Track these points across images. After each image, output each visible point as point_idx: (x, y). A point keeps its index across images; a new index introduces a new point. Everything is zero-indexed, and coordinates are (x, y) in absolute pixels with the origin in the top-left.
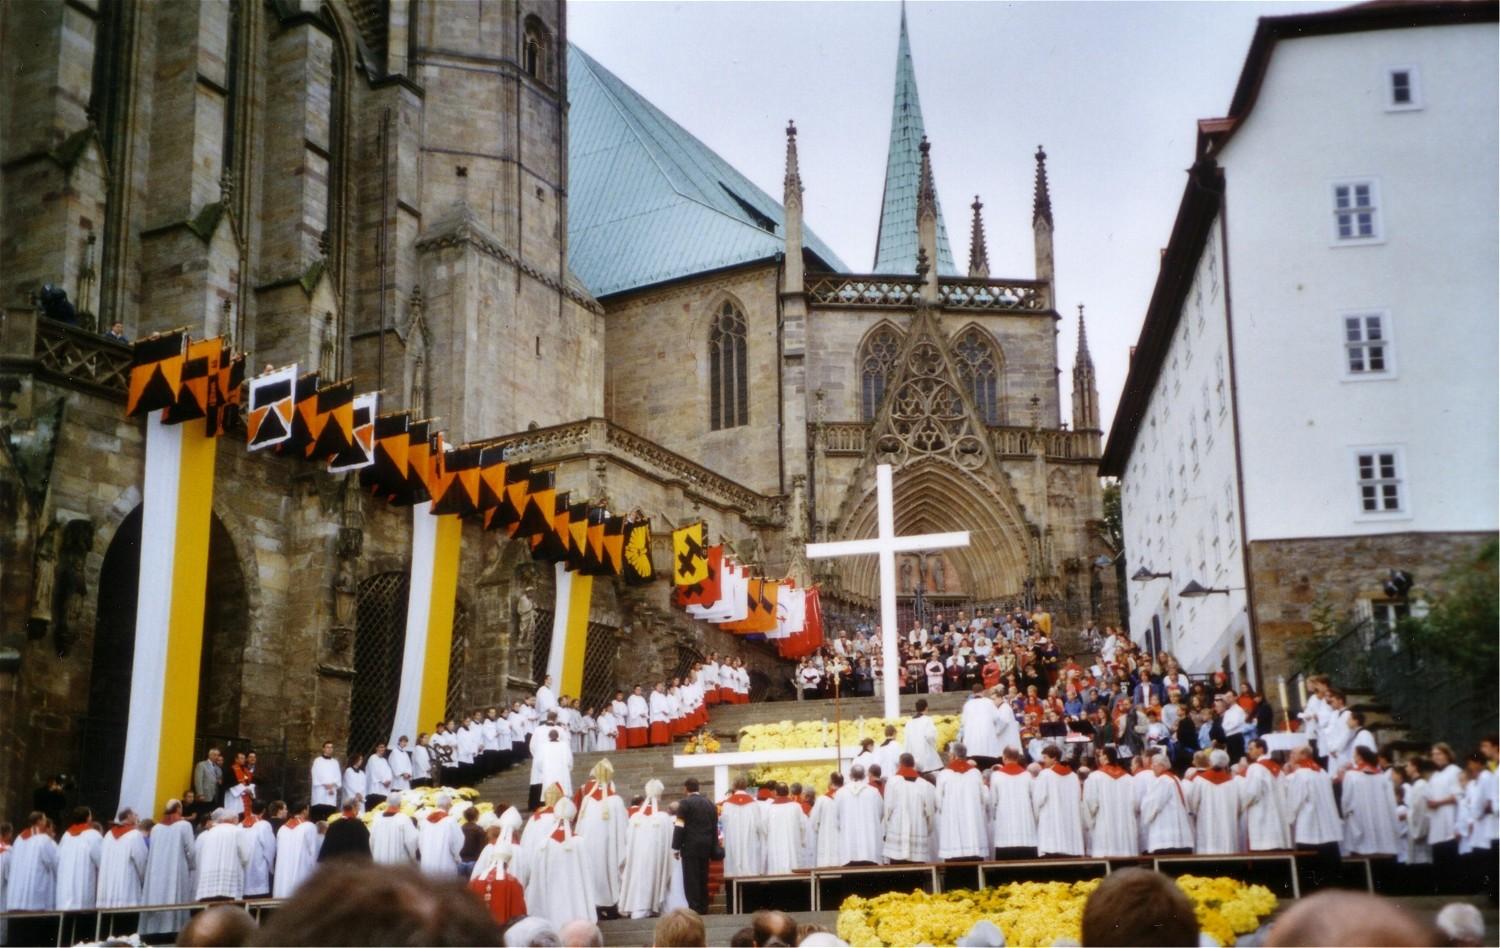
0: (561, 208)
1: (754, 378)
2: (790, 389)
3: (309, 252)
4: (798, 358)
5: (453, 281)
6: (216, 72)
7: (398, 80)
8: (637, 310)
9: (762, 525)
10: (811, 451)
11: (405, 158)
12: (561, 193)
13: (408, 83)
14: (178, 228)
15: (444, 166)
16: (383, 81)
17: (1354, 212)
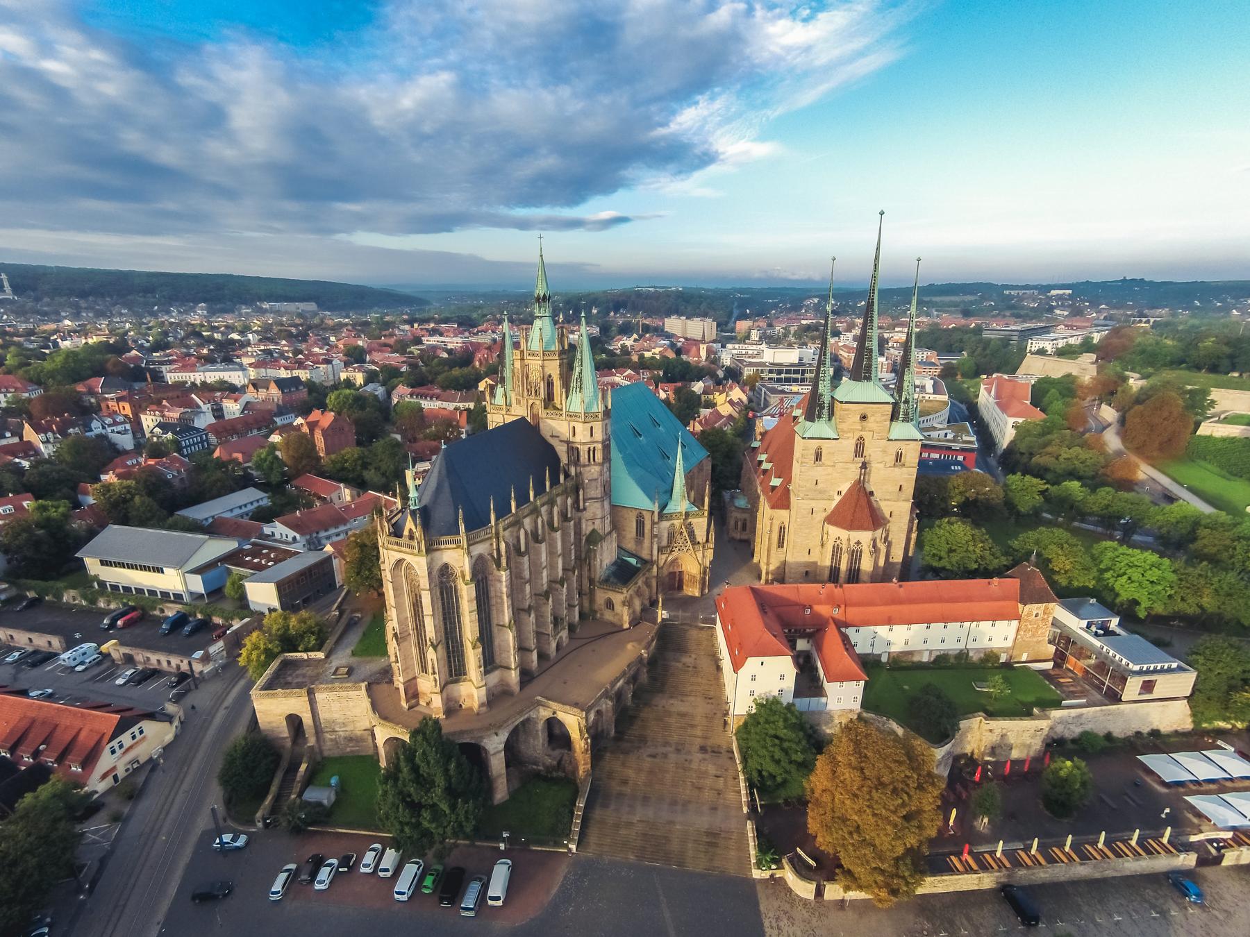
4: (656, 536)
11: (584, 526)
15: (590, 523)
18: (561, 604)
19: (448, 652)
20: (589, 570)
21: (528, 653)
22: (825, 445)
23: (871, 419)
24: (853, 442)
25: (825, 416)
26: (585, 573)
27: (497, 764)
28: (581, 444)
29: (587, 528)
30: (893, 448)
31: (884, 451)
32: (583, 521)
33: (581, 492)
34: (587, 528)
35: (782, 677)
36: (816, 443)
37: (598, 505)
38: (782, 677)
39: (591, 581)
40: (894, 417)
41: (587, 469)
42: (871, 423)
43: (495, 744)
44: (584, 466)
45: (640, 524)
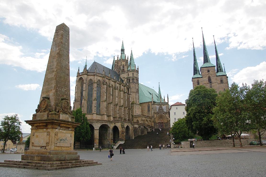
5: (133, 106)
8: (143, 104)
9: (151, 119)
10: (154, 114)
11: (130, 99)
12: (139, 99)
14: (121, 106)
15: (132, 99)
17: (175, 113)
19: (88, 105)
20: (132, 112)
21: (110, 117)
23: (210, 71)
25: (198, 73)
26: (131, 113)
27: (96, 134)
28: (130, 77)
30: (219, 78)
33: (130, 89)
36: (196, 80)
39: (132, 116)
40: (218, 71)
41: (132, 84)
42: (211, 72)
43: (97, 126)
44: (131, 83)
45: (149, 107)
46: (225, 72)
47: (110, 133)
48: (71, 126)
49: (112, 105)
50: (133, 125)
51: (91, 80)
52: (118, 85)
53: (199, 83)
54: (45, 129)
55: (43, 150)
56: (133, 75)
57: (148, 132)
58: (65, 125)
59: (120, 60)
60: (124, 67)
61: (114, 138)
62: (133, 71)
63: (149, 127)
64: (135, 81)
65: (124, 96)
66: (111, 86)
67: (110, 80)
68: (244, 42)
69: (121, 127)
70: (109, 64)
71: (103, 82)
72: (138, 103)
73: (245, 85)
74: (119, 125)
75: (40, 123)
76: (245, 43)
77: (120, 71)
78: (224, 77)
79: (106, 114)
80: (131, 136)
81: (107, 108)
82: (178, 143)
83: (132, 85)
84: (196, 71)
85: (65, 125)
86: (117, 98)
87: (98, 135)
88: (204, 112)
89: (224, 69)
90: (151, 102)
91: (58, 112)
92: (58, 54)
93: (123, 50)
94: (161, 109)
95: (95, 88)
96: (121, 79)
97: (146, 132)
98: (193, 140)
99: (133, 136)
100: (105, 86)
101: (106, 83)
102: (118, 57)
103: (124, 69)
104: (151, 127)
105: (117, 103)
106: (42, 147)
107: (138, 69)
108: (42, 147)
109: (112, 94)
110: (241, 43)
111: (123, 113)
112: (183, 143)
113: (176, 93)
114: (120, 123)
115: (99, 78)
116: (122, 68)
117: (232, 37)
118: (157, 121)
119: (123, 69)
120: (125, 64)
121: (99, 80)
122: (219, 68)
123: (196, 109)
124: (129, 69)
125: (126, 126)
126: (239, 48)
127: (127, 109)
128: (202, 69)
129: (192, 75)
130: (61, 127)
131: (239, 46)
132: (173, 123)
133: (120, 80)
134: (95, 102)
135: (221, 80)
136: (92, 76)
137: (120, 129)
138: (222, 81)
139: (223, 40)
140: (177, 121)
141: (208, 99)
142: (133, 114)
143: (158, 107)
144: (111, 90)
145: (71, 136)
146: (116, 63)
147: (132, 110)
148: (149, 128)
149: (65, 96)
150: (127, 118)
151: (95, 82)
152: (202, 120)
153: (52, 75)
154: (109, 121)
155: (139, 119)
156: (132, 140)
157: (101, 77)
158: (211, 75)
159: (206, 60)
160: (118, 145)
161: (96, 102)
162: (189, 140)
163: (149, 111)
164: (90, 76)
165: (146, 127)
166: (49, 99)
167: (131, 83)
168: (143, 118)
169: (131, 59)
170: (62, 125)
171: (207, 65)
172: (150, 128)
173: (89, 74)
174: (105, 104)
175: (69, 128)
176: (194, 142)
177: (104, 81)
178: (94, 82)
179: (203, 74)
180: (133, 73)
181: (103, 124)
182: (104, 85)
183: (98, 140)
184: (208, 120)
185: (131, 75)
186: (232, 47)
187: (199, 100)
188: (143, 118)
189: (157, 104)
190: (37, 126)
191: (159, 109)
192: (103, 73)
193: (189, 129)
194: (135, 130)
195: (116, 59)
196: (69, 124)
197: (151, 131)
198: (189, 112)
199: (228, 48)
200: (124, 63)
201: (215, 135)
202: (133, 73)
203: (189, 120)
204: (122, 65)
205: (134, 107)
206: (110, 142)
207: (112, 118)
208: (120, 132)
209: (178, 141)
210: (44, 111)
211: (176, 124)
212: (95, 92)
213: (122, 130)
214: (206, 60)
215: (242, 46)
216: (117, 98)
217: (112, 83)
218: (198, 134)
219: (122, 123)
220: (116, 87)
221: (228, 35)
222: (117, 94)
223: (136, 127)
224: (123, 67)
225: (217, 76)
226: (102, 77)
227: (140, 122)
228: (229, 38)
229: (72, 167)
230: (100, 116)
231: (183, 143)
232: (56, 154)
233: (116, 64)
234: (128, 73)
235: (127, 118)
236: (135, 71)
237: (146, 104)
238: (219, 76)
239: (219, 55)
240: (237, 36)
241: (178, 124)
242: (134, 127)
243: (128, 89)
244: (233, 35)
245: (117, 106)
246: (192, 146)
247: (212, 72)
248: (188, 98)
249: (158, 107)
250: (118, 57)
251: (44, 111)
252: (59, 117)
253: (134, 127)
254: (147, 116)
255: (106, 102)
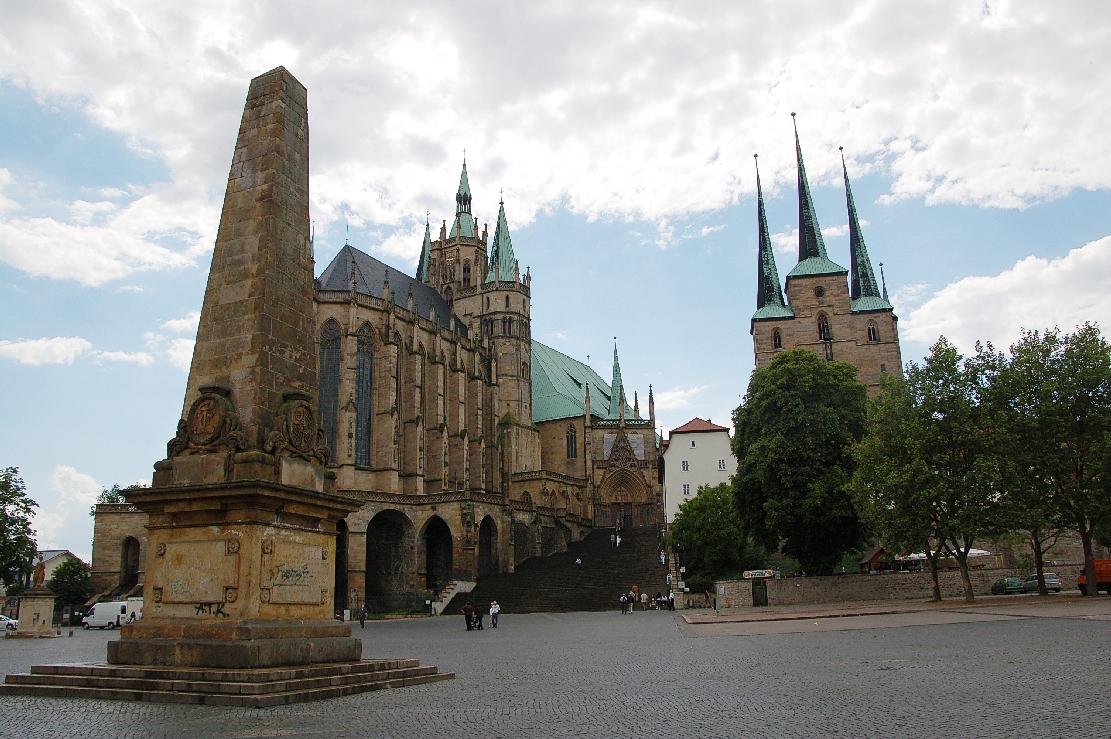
0: (531, 409)
1: (578, 446)
2: (588, 452)
3: (480, 433)
6: (462, 399)
7: (494, 385)
9: (580, 487)
12: (531, 405)
13: (496, 385)
14: (456, 435)
15: (504, 404)
16: (490, 384)
17: (685, 466)
18: (460, 464)
21: (411, 481)
22: (780, 325)
23: (828, 293)
24: (814, 319)
26: (498, 465)
28: (495, 313)
29: (500, 410)
30: (862, 323)
31: (851, 327)
32: (496, 398)
33: (494, 364)
34: (500, 410)
35: (722, 464)
36: (771, 325)
37: (513, 384)
38: (722, 464)
39: (503, 475)
40: (856, 295)
42: (828, 298)
44: (498, 337)
45: (571, 440)
46: (886, 296)
47: (412, 548)
48: (324, 515)
49: (420, 429)
50: (510, 514)
51: (332, 320)
52: (445, 346)
53: (780, 341)
54: (215, 529)
55: (210, 619)
56: (507, 306)
57: (569, 544)
58: (301, 511)
59: (452, 239)
60: (469, 272)
61: (429, 566)
62: (509, 285)
63: (578, 523)
64: (515, 328)
65: (471, 393)
66: (415, 347)
67: (411, 322)
68: (951, 177)
69: (458, 522)
70: (404, 254)
71: (383, 330)
72: (525, 420)
73: (985, 349)
74: (450, 513)
75: (191, 501)
76: (954, 182)
77: (451, 285)
78: (883, 316)
79: (394, 466)
80: (501, 559)
81: (401, 437)
82: (701, 588)
83: (504, 348)
84: (766, 292)
85: (301, 511)
86: (440, 402)
87: (363, 557)
88: (810, 461)
89: (884, 289)
90: (584, 416)
91: (273, 452)
92: (267, 198)
93: (464, 199)
94: (622, 448)
95: (352, 355)
96: (457, 320)
97: (564, 543)
98: (767, 573)
99: (512, 560)
100: (393, 349)
101: (397, 334)
102: (443, 229)
103: (469, 280)
104: (584, 522)
105: (441, 420)
106: (205, 604)
107: (528, 278)
108: (202, 606)
109: (419, 382)
110: (940, 179)
111: (466, 465)
112: (722, 588)
113: (690, 383)
114: (456, 505)
115: (367, 315)
116: (459, 275)
117: (903, 153)
118: (607, 498)
119: (467, 280)
120: (472, 258)
121: (367, 324)
122: (863, 280)
123: (782, 445)
124: (491, 277)
125: (479, 518)
126: (931, 200)
127: (483, 445)
128: (793, 282)
129: (751, 309)
130: (286, 516)
131: (932, 191)
132: (680, 506)
133: (452, 323)
134: (348, 414)
135: (869, 330)
136: (335, 307)
137: (456, 532)
138: (873, 336)
139: (869, 165)
140: (693, 495)
141: (829, 405)
142: (506, 469)
143: (609, 437)
144: (418, 367)
145: (323, 558)
146: (436, 253)
147: (502, 453)
148: (575, 525)
149: (297, 384)
150: (483, 486)
151: (350, 330)
152: (805, 493)
153: (243, 291)
154: (407, 497)
155: (534, 490)
156: (506, 574)
157: (373, 309)
158: (828, 310)
159: (810, 244)
160: (448, 596)
161: (354, 415)
162: (747, 574)
163: (572, 452)
164: (326, 306)
165: (563, 520)
166: (228, 393)
167: (498, 337)
168: (550, 486)
169: (497, 234)
170: (292, 509)
171: (812, 266)
172: (579, 525)
173: (321, 295)
174: (390, 424)
175: (317, 520)
176: (769, 583)
177: (388, 327)
178: (347, 329)
179: (794, 303)
180: (507, 297)
181: (386, 507)
182: (385, 344)
183: (363, 575)
184: (830, 492)
185: (497, 303)
186: (904, 196)
187: (790, 411)
188: (550, 486)
189: (604, 427)
190: (174, 516)
191: (615, 449)
192: (385, 294)
193: (747, 528)
194: (519, 533)
195: (435, 236)
196: (319, 503)
197: (582, 535)
198: (749, 459)
199: (886, 199)
200: (468, 254)
201: (853, 553)
202: (507, 297)
203: (748, 492)
204: (461, 261)
205: (513, 436)
206: (412, 586)
207: (420, 483)
208: (455, 544)
209: (697, 579)
210: (208, 447)
211: (694, 511)
212: (352, 375)
213: (465, 533)
214: (810, 244)
215: (945, 193)
216: (440, 402)
217: (420, 336)
218: (784, 550)
219: (463, 505)
220: (438, 353)
221: (887, 143)
222: (440, 383)
223: (521, 523)
224: (467, 270)
225: (854, 313)
226: (378, 310)
227: (538, 501)
228: (892, 157)
229: (346, 693)
230: (371, 476)
231: (722, 588)
232: (270, 634)
233: (435, 255)
234: (485, 295)
235: (483, 486)
236: (517, 287)
237: (559, 428)
238: (862, 312)
239: (861, 223)
240: (923, 149)
241: (703, 506)
242: (513, 521)
243: (487, 362)
244: (908, 143)
245: (442, 433)
246: (760, 600)
247: (835, 296)
248: (741, 402)
249: (609, 437)
250: (443, 229)
251: (208, 447)
252: (278, 473)
253: (513, 521)
254: (566, 477)
255: (395, 416)
